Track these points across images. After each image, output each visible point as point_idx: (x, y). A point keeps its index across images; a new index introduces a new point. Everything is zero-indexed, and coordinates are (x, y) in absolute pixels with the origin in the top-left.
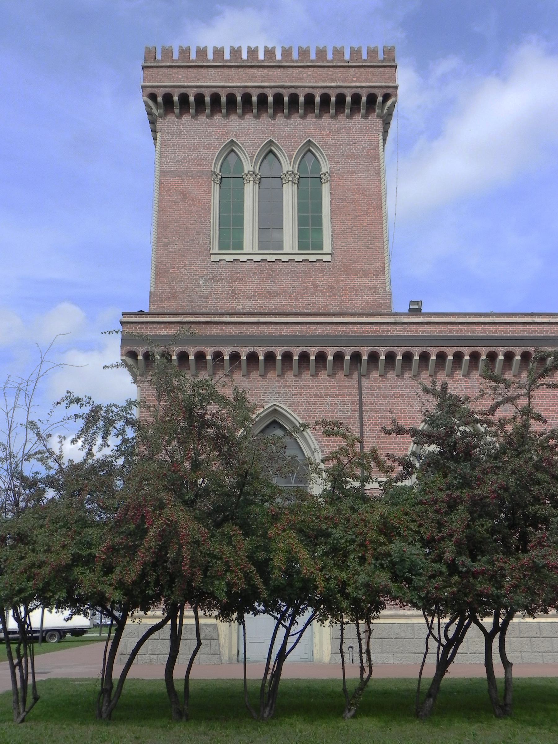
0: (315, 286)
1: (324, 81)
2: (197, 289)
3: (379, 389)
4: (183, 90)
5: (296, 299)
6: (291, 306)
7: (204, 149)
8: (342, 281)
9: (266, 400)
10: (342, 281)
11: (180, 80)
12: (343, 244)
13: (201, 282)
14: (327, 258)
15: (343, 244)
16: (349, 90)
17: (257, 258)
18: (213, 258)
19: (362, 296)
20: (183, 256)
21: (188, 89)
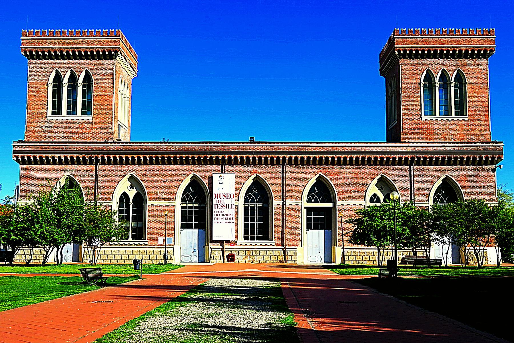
0: (86, 129)
1: (92, 45)
2: (43, 131)
3: (106, 169)
4: (36, 49)
5: (79, 135)
6: (77, 137)
7: (46, 73)
8: (96, 127)
9: (65, 173)
10: (96, 127)
11: (35, 45)
12: (97, 113)
13: (44, 128)
14: (91, 118)
15: (97, 113)
16: (101, 49)
17: (64, 118)
18: (49, 118)
19: (103, 133)
20: (37, 117)
21: (39, 49)
